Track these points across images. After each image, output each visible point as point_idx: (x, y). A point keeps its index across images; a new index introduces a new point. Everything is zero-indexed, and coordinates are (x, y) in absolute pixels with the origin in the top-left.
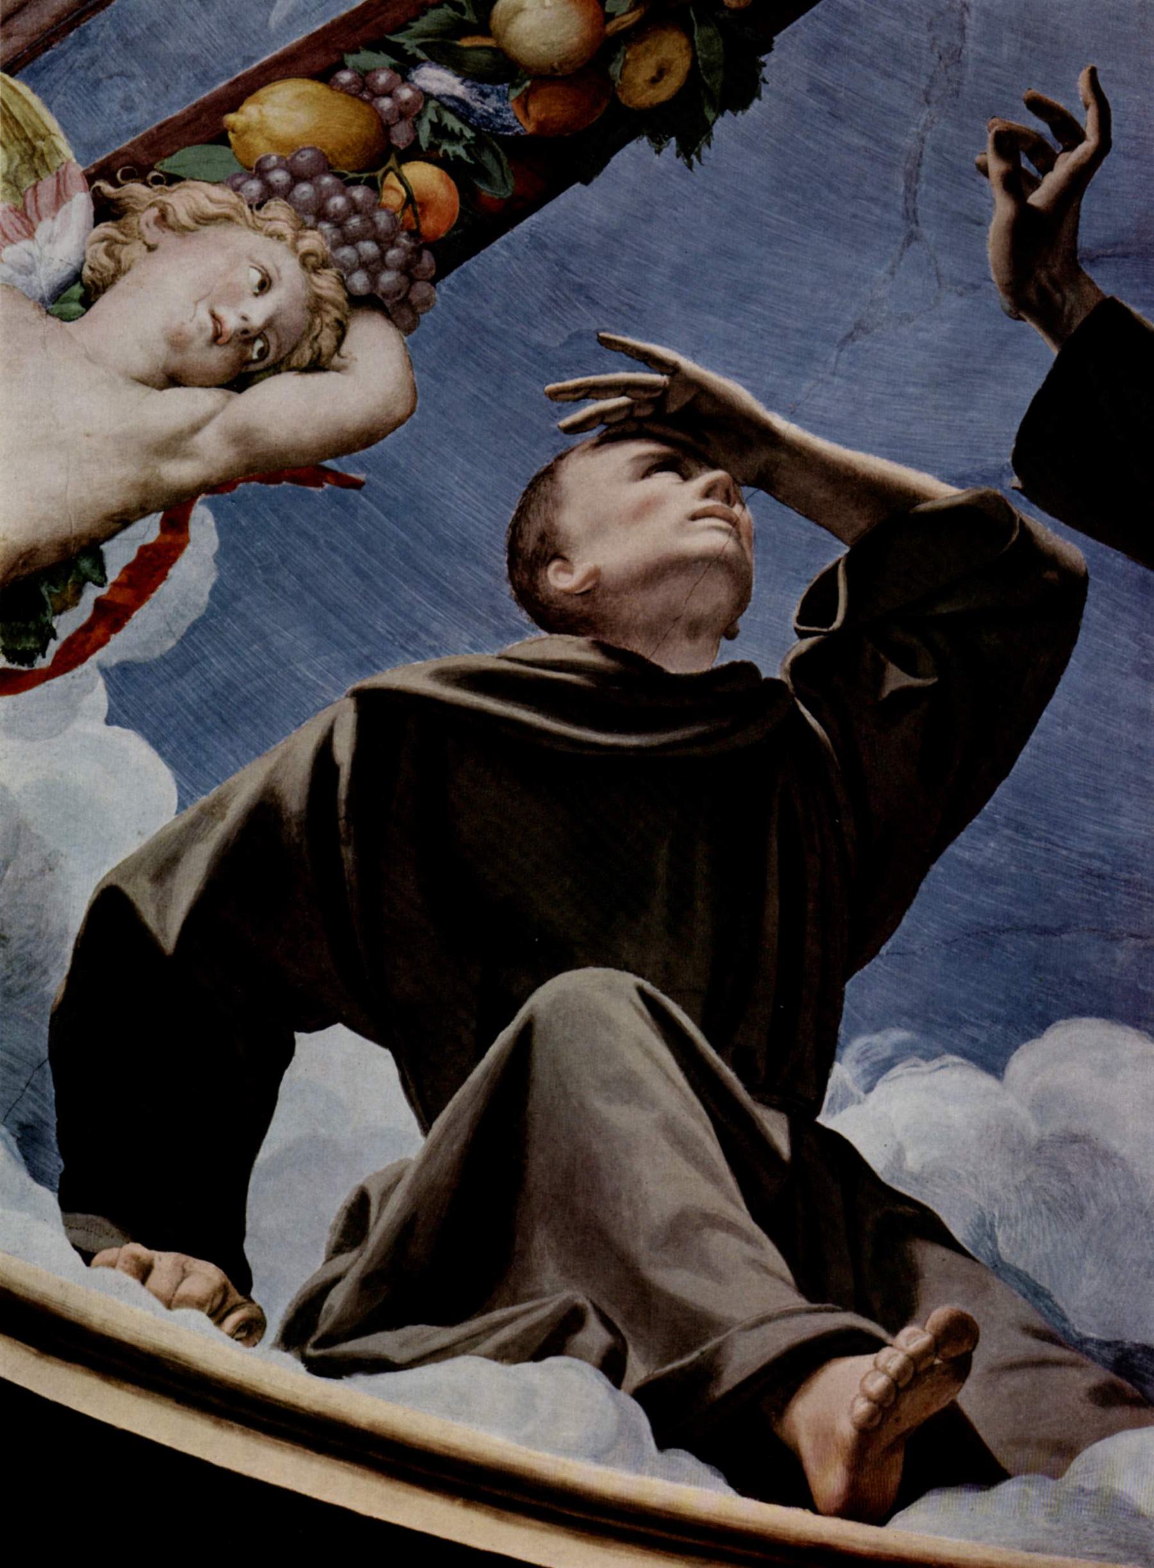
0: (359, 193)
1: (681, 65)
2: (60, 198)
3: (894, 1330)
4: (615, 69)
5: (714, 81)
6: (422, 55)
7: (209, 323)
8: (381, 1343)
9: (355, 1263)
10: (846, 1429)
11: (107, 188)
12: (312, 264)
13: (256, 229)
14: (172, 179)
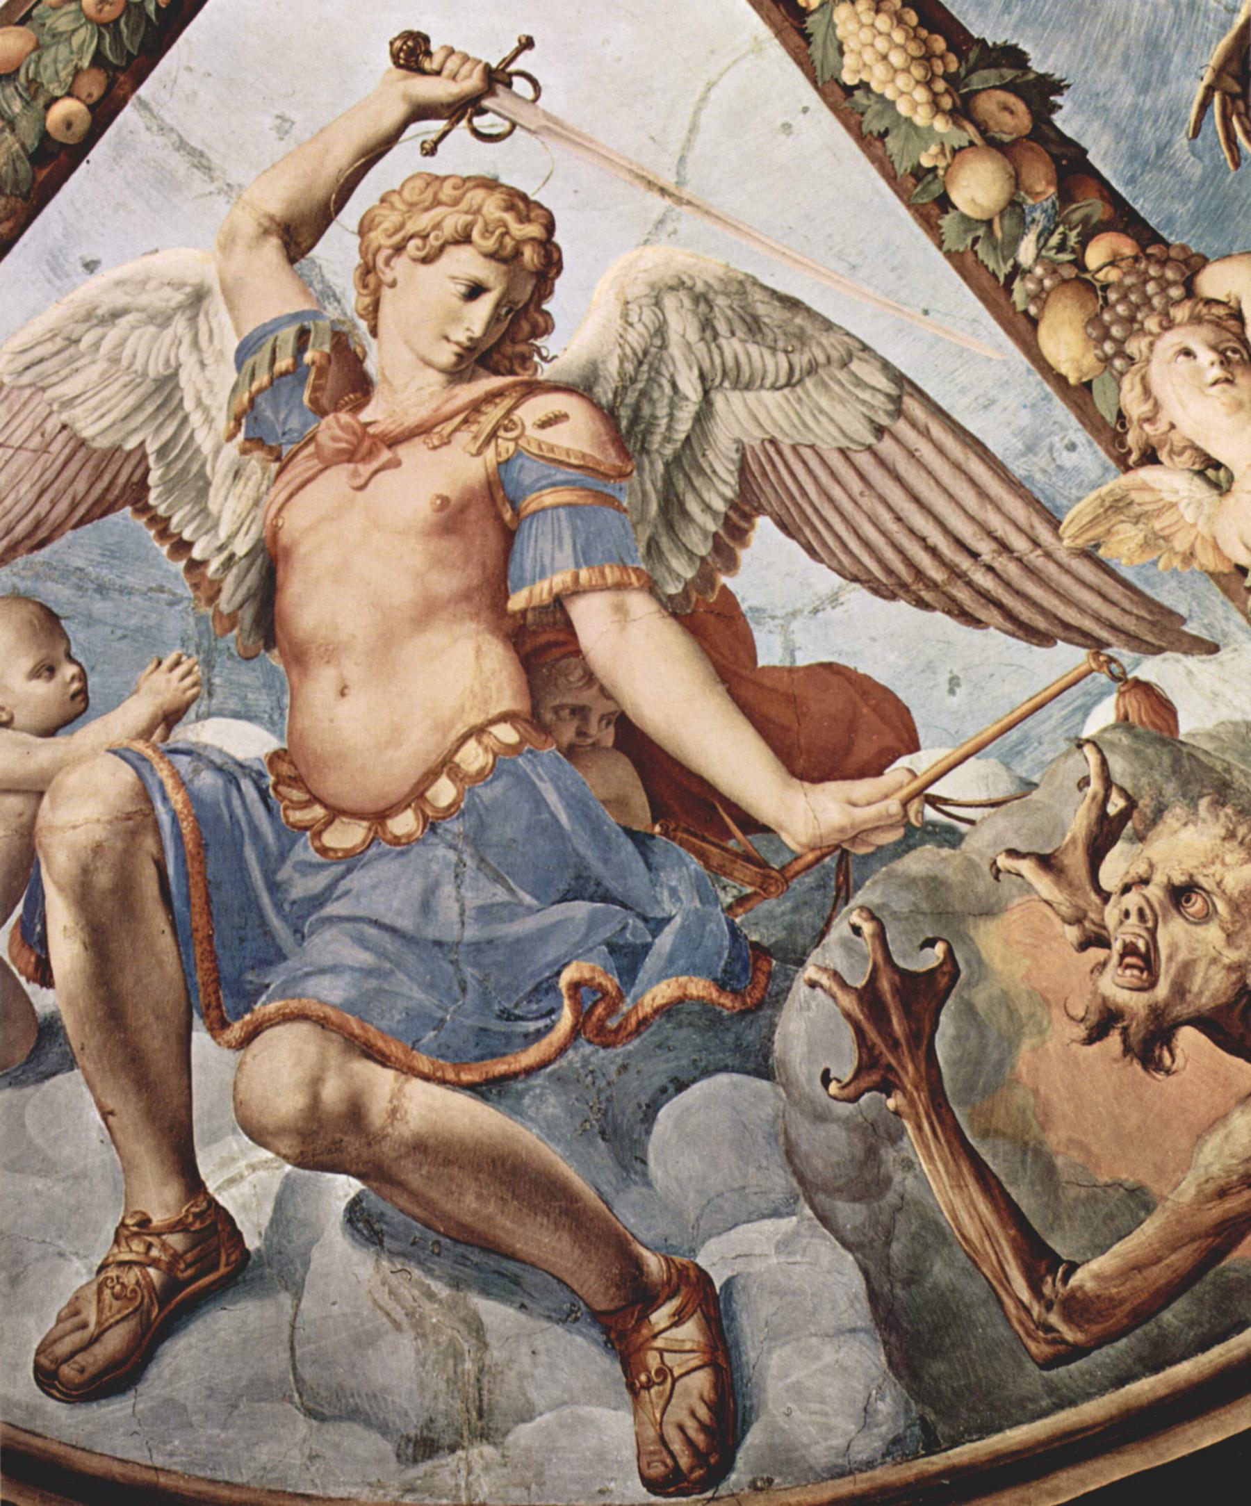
0: (1113, 296)
2: (1145, 487)
4: (1007, 138)
5: (1009, 74)
6: (1011, 262)
7: (1219, 387)
11: (1134, 457)
12: (1168, 324)
13: (1148, 361)
14: (1121, 416)
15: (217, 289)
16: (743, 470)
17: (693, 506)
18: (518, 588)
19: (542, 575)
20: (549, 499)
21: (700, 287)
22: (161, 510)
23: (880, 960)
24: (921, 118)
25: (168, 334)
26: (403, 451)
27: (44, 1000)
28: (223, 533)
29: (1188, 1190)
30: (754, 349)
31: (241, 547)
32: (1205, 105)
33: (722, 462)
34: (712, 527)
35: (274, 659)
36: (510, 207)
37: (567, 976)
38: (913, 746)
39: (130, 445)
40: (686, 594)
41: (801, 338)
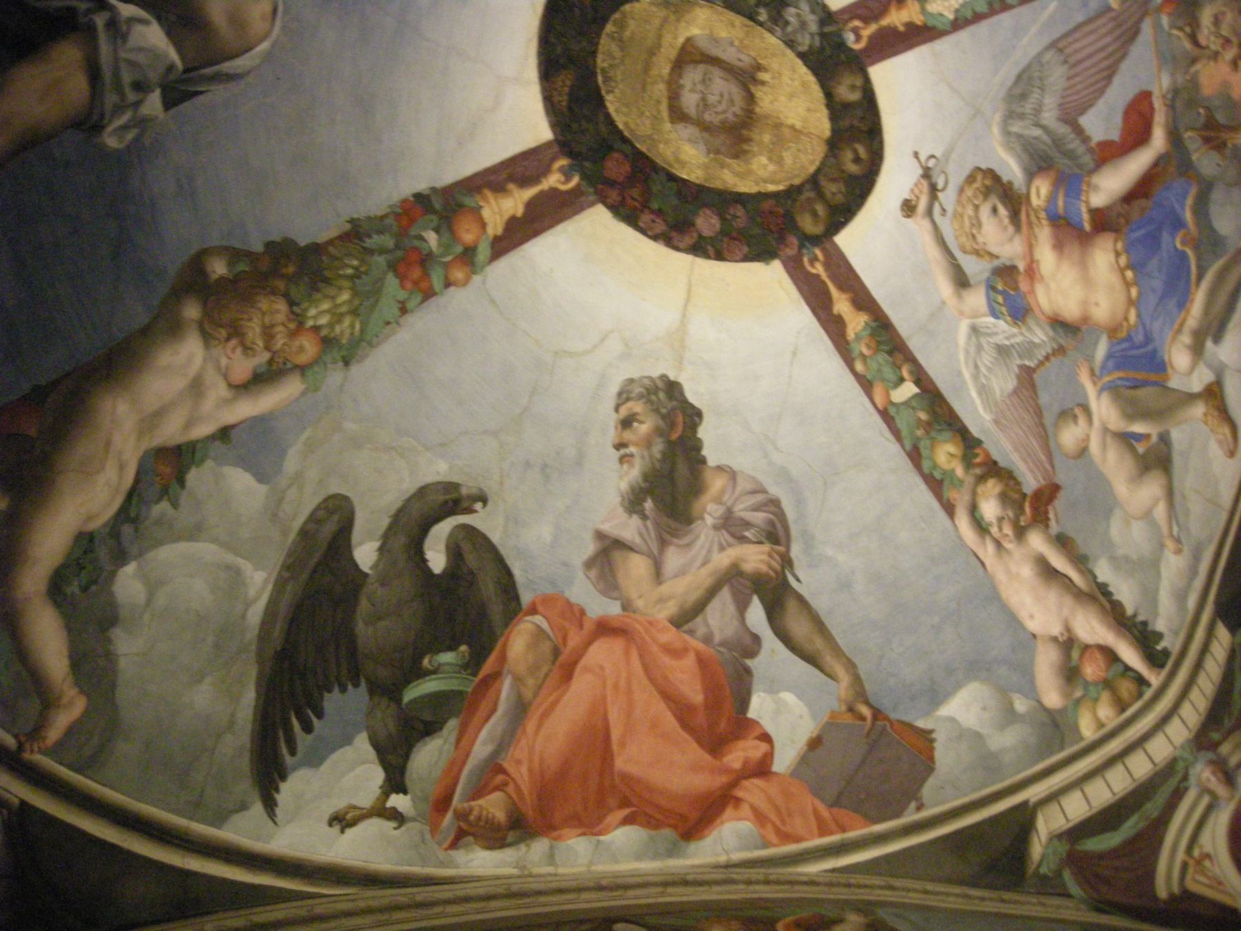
15: (972, 321)
16: (1066, 122)
17: (1071, 146)
18: (1082, 226)
20: (1060, 203)
21: (1007, 113)
22: (1036, 362)
23: (1198, 132)
25: (985, 346)
27: (1154, 439)
28: (1045, 339)
30: (1032, 100)
31: (1051, 333)
33: (1063, 130)
35: (1084, 328)
39: (1016, 370)
40: (1094, 160)
41: (1030, 78)
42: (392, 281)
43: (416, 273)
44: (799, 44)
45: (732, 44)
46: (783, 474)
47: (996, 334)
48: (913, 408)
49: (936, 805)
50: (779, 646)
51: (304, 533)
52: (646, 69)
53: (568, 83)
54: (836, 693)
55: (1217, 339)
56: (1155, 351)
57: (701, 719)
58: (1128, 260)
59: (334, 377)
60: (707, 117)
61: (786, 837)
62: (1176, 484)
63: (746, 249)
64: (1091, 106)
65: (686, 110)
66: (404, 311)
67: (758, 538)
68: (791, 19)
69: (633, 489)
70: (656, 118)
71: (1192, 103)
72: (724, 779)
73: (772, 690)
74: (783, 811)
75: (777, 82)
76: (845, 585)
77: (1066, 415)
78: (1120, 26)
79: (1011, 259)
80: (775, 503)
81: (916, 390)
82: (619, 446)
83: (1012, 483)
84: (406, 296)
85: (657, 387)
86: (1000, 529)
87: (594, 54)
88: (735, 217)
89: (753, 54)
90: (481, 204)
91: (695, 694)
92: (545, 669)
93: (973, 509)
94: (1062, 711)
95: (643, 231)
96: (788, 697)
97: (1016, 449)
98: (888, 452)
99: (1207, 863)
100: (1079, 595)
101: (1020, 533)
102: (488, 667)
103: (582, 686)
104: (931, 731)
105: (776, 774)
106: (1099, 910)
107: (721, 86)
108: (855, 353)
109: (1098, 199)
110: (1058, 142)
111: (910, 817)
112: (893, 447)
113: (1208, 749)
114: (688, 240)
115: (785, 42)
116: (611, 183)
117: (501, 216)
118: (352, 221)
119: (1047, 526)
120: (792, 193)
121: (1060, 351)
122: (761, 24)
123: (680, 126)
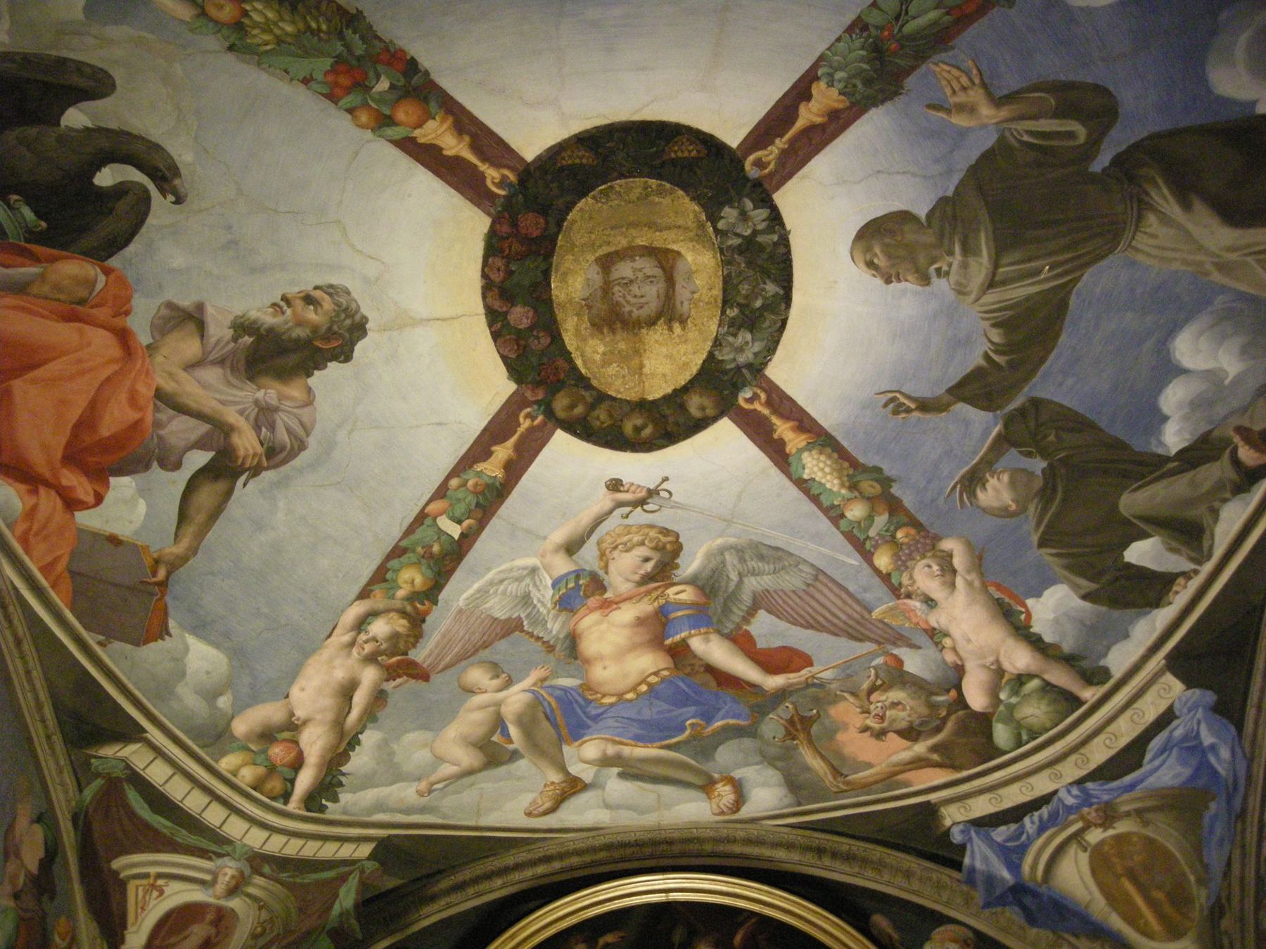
0: (904, 547)
1: (871, 483)
3: (1232, 442)
5: (875, 475)
8: (1205, 549)
9: (1183, 549)
10: (1256, 455)
12: (924, 556)
13: (914, 568)
14: (900, 584)
17: (735, 609)
19: (677, 634)
20: (680, 613)
24: (835, 489)
25: (523, 584)
26: (621, 605)
27: (511, 747)
28: (554, 632)
29: (884, 765)
30: (760, 564)
31: (562, 636)
32: (954, 487)
33: (746, 598)
34: (741, 614)
35: (578, 662)
36: (661, 533)
37: (688, 722)
38: (811, 665)
40: (731, 632)
41: (780, 559)
42: (327, 63)
43: (344, 81)
44: (720, 350)
45: (693, 292)
46: (329, 446)
47: (539, 590)
48: (439, 538)
49: (110, 657)
50: (182, 487)
51: (63, 61)
52: (634, 225)
53: (584, 161)
54: (163, 543)
55: (622, 775)
56: (589, 727)
57: (88, 439)
58: (656, 683)
59: (212, 42)
60: (616, 289)
61: (24, 541)
62: (480, 775)
63: (514, 356)
64: (779, 618)
65: (613, 270)
66: (306, 81)
67: (265, 439)
68: (739, 340)
69: (255, 322)
70: (592, 246)
71: (817, 701)
72: (47, 475)
73: (142, 492)
74: (45, 532)
75: (677, 340)
76: (259, 525)
77: (495, 669)
78: (858, 623)
79: (610, 585)
80: (302, 446)
81: (456, 537)
82: (284, 298)
83: (411, 639)
84: (319, 79)
85: (353, 316)
86: (366, 642)
87: (622, 176)
88: (538, 338)
89: (693, 313)
90: (437, 118)
91: (108, 427)
92: (62, 297)
93: (373, 614)
94: (233, 738)
95: (485, 263)
96: (142, 507)
97: (444, 636)
98: (391, 527)
99: (155, 894)
100: (338, 723)
101: (371, 659)
102: (38, 249)
103: (64, 333)
104: (170, 635)
105: (73, 515)
106: (75, 819)
107: (651, 293)
108: (465, 477)
109: (697, 644)
110: (733, 597)
111: (91, 639)
112: (397, 532)
113: (252, 867)
114: (497, 305)
115: (716, 339)
116: (514, 224)
117: (436, 137)
118: (360, 12)
119: (387, 680)
120: (583, 382)
121: (550, 648)
122: (723, 313)
123: (596, 268)
